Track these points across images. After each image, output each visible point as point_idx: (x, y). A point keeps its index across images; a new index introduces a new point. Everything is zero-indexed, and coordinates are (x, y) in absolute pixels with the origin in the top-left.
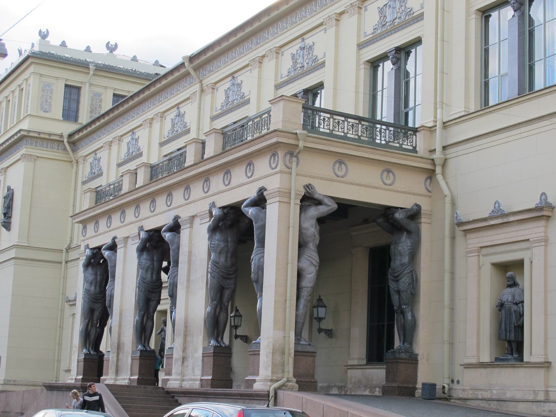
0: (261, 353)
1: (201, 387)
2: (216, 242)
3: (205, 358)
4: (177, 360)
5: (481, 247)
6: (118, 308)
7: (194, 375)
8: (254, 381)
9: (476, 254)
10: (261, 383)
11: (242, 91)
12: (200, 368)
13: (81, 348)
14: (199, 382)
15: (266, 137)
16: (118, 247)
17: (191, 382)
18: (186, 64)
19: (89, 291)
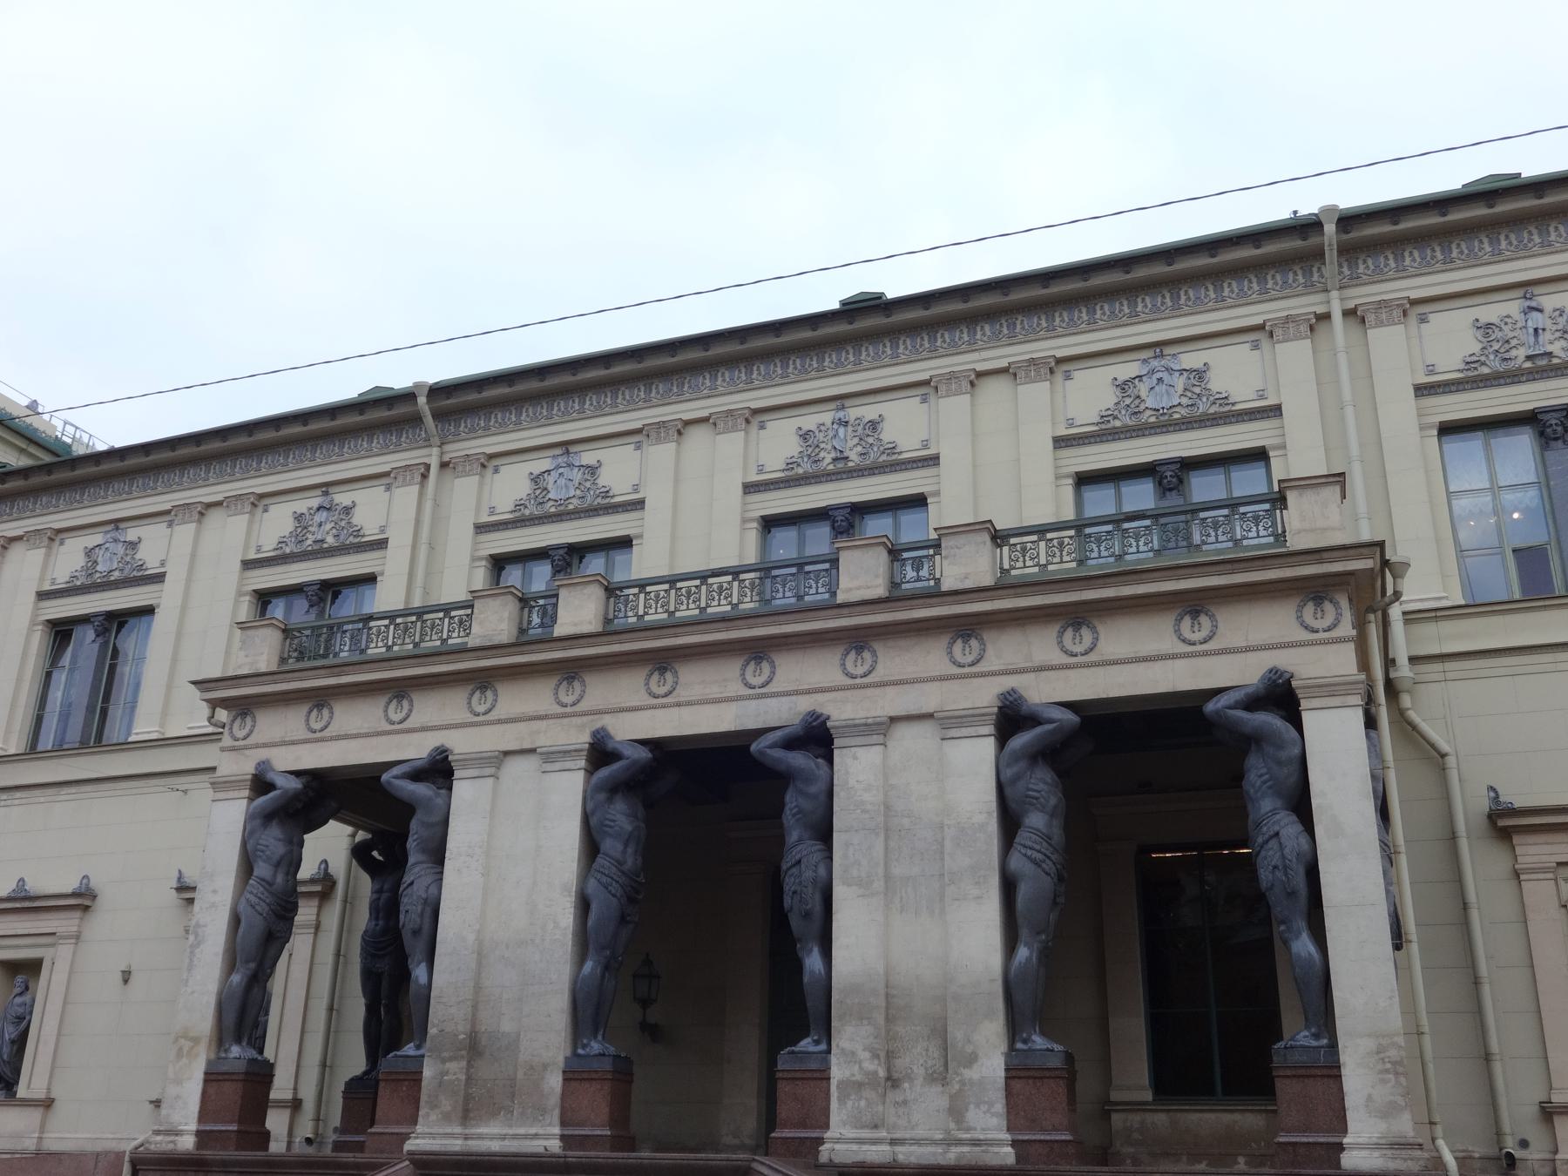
0: (1344, 1072)
1: (1018, 1161)
2: (1041, 786)
3: (1017, 1085)
4: (850, 1087)
5: (1559, 864)
6: (471, 937)
7: (968, 1130)
8: (1340, 1148)
9: (1551, 876)
10: (1376, 1154)
11: (601, 482)
12: (1000, 1107)
13: (214, 1044)
14: (1010, 1149)
15: (1325, 555)
16: (457, 774)
17: (966, 1149)
18: (422, 400)
19: (270, 884)
